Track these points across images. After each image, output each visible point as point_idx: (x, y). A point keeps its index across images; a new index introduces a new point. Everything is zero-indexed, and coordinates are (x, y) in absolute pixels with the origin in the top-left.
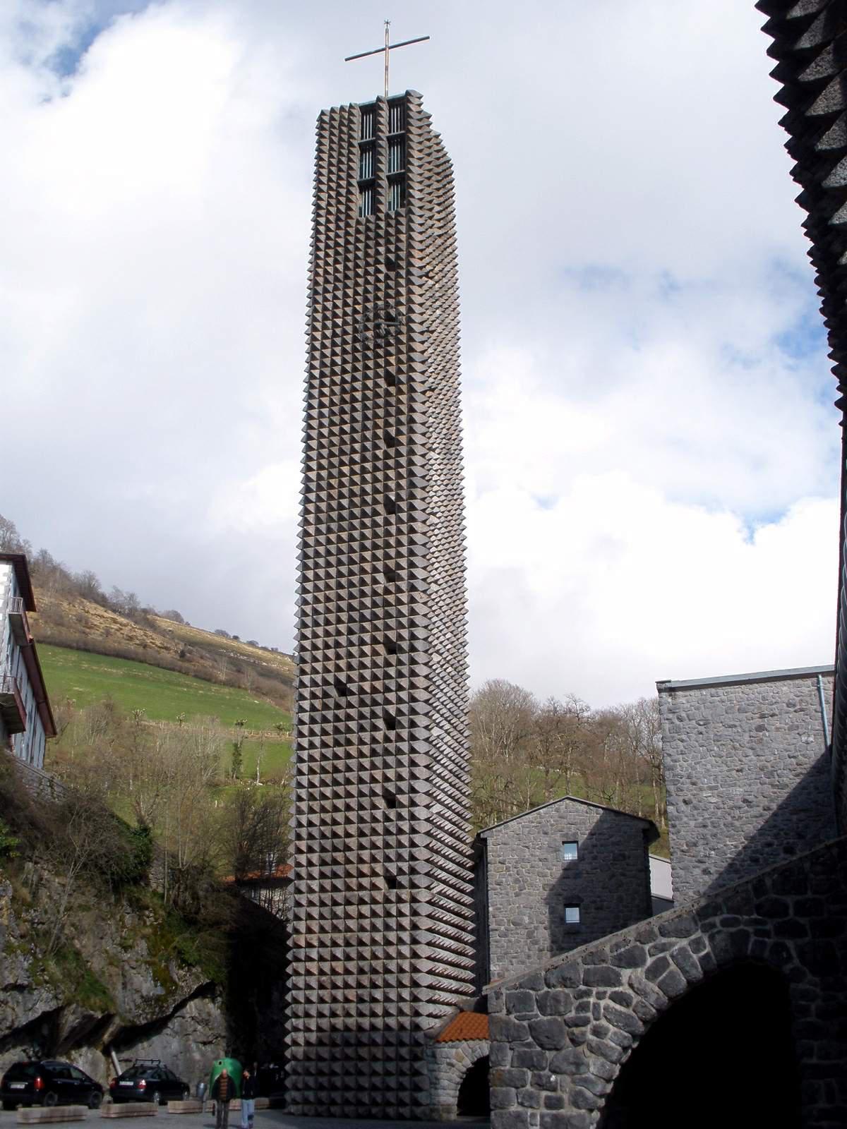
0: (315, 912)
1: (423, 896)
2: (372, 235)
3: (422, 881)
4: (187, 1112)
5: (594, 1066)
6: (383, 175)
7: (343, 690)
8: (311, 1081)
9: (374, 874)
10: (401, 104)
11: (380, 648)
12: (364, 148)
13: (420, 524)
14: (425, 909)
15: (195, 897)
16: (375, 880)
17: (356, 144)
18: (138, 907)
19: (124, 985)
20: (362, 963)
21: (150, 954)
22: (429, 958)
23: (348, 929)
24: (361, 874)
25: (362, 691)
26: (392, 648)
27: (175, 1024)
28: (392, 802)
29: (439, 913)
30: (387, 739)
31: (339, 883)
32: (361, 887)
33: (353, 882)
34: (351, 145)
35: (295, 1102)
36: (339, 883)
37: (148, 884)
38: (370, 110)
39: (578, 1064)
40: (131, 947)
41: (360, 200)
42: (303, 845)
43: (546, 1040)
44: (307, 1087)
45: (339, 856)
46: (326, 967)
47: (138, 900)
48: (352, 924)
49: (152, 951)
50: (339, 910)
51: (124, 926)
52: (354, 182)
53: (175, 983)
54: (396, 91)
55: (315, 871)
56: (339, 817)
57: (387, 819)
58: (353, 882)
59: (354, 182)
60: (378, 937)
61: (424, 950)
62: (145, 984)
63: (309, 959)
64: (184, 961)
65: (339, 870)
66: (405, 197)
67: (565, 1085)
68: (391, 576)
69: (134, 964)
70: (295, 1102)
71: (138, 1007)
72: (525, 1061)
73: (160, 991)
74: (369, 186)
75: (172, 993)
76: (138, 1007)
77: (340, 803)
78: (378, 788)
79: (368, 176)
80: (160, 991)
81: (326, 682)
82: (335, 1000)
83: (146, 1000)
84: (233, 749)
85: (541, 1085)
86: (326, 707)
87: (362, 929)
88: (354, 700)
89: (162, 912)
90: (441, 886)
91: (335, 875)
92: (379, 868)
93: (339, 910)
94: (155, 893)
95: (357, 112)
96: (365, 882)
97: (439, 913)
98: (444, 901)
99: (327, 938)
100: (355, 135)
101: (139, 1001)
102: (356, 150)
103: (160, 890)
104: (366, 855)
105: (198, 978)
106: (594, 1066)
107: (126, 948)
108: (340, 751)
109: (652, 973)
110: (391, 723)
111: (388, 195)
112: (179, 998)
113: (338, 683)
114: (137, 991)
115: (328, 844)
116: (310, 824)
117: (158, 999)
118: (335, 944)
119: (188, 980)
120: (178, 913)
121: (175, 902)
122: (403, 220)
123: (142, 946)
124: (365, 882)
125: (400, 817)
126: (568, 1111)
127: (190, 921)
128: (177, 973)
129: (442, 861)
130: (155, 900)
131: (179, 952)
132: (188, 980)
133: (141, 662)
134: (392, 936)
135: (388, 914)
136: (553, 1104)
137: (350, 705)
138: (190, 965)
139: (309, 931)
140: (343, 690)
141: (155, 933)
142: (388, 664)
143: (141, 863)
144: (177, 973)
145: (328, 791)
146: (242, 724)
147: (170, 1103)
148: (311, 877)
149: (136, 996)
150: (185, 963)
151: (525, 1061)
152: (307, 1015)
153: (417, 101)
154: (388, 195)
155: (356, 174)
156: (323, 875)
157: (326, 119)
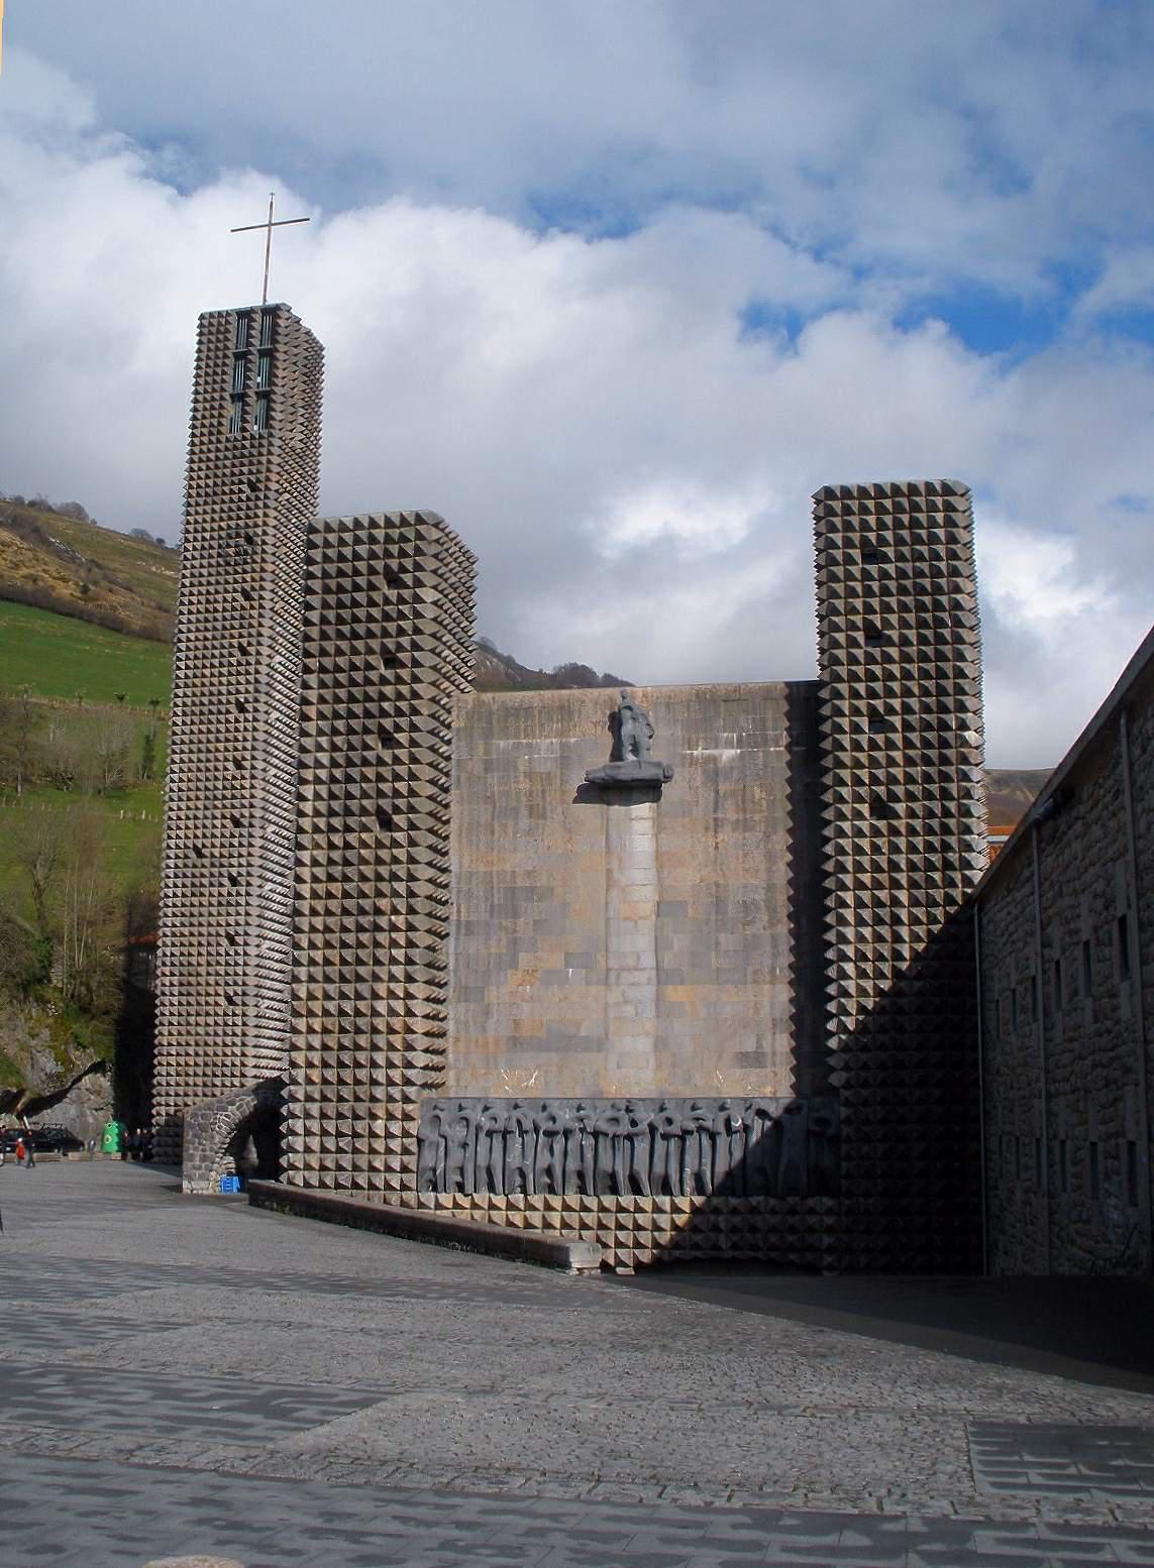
0: (175, 1020)
1: (251, 1012)
2: (239, 453)
3: (251, 1001)
4: (81, 1160)
5: (217, 1139)
6: (250, 392)
7: (200, 855)
8: (169, 1140)
9: (217, 994)
10: (272, 312)
11: (228, 823)
12: (238, 356)
13: (262, 724)
14: (252, 1021)
15: (89, 988)
16: (217, 998)
17: (230, 355)
18: (42, 1001)
19: (33, 1066)
20: (206, 1059)
21: (52, 1040)
22: (255, 1056)
23: (198, 1034)
24: (208, 994)
25: (213, 856)
26: (237, 823)
27: (72, 1095)
28: (232, 942)
29: (264, 1022)
30: (230, 894)
31: (192, 1000)
32: (207, 1003)
33: (202, 1000)
34: (226, 356)
35: (158, 1155)
36: (192, 1000)
37: (50, 981)
38: (245, 315)
39: (213, 1137)
40: (37, 1035)
41: (231, 410)
42: (167, 970)
43: (203, 1129)
44: (167, 1145)
45: (192, 980)
46: (182, 1060)
47: (42, 996)
48: (200, 1030)
49: (54, 1037)
50: (192, 1020)
51: (31, 1018)
52: (226, 395)
53: (74, 1064)
54: (271, 301)
55: (175, 990)
56: (194, 951)
57: (228, 954)
58: (202, 1000)
59: (226, 395)
60: (219, 1040)
61: (250, 1051)
62: (50, 1065)
63: (170, 1054)
64: (79, 1044)
65: (192, 990)
66: (268, 420)
67: (208, 1144)
68: (239, 766)
69: (39, 1049)
70: (158, 1155)
71: (43, 1082)
72: (195, 1136)
73: (60, 1069)
74: (239, 398)
75: (71, 1070)
76: (43, 1082)
77: (194, 940)
78: (222, 931)
79: (239, 390)
80: (60, 1069)
81: (186, 847)
82: (187, 1084)
83: (50, 1076)
84: (143, 742)
85: (200, 1144)
86: (186, 866)
87: (207, 1034)
88: (206, 862)
89: (61, 1005)
90: (267, 1003)
91: (189, 994)
92: (221, 991)
93: (192, 1020)
94: (55, 988)
95: (233, 319)
96: (211, 1000)
97: (264, 1022)
98: (269, 1013)
99: (182, 1040)
100: (229, 344)
101: (44, 1078)
102: (230, 361)
103: (60, 985)
104: (211, 980)
105: (91, 1058)
106: (217, 1139)
107: (33, 1037)
108: (195, 900)
109: (238, 1109)
110: (234, 881)
111: (256, 407)
112: (75, 1075)
113: (195, 848)
114: (42, 1070)
115: (185, 970)
116: (172, 955)
117: (58, 1075)
118: (188, 1044)
119: (83, 1059)
120: (74, 1006)
121: (73, 996)
122: (265, 442)
123: (46, 1033)
124: (211, 1000)
125: (237, 953)
126: (208, 1153)
127: (85, 1009)
128: (74, 1054)
129: (268, 983)
130: (56, 995)
131: (76, 1037)
132: (83, 1059)
133: (30, 605)
134: (228, 1040)
135: (226, 1024)
136: (203, 1150)
137: (203, 866)
138: (84, 1047)
139: (170, 1034)
140: (200, 855)
141: (56, 1022)
142: (232, 836)
143: (44, 967)
144: (74, 1054)
145: (186, 931)
146: (158, 702)
147: (70, 1154)
148: (172, 995)
149: (42, 1074)
150: (81, 1046)
151: (195, 1136)
152: (168, 1095)
153: (287, 315)
154: (256, 407)
155: (228, 387)
156: (181, 994)
157: (205, 322)
